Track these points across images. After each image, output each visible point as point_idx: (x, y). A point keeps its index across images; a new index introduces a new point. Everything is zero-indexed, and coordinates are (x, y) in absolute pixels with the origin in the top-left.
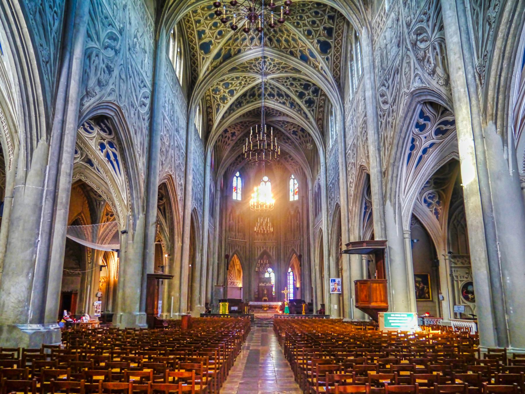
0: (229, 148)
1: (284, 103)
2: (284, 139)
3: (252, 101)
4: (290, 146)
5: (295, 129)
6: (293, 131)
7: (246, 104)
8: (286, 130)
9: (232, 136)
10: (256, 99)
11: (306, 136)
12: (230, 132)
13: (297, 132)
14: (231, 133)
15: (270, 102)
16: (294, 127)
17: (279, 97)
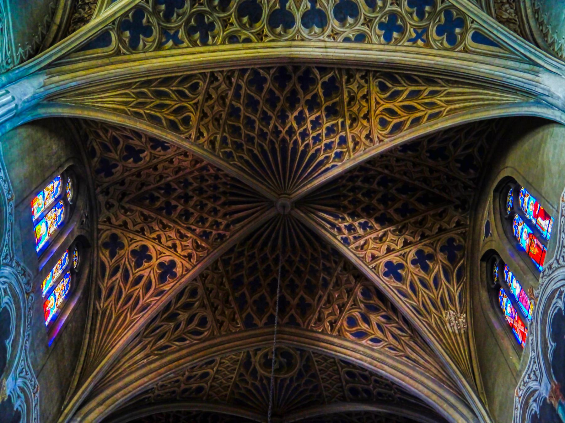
0: (141, 320)
1: (361, 38)
2: (352, 322)
3: (248, 40)
4: (378, 347)
5: (394, 258)
6: (389, 264)
7: (223, 43)
8: (362, 259)
9: (162, 278)
10: (260, 36)
11: (436, 281)
12: (155, 262)
13: (401, 266)
14: (161, 265)
15: (312, 44)
16: (389, 250)
17: (342, 21)
